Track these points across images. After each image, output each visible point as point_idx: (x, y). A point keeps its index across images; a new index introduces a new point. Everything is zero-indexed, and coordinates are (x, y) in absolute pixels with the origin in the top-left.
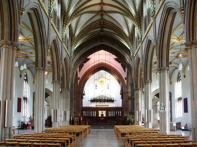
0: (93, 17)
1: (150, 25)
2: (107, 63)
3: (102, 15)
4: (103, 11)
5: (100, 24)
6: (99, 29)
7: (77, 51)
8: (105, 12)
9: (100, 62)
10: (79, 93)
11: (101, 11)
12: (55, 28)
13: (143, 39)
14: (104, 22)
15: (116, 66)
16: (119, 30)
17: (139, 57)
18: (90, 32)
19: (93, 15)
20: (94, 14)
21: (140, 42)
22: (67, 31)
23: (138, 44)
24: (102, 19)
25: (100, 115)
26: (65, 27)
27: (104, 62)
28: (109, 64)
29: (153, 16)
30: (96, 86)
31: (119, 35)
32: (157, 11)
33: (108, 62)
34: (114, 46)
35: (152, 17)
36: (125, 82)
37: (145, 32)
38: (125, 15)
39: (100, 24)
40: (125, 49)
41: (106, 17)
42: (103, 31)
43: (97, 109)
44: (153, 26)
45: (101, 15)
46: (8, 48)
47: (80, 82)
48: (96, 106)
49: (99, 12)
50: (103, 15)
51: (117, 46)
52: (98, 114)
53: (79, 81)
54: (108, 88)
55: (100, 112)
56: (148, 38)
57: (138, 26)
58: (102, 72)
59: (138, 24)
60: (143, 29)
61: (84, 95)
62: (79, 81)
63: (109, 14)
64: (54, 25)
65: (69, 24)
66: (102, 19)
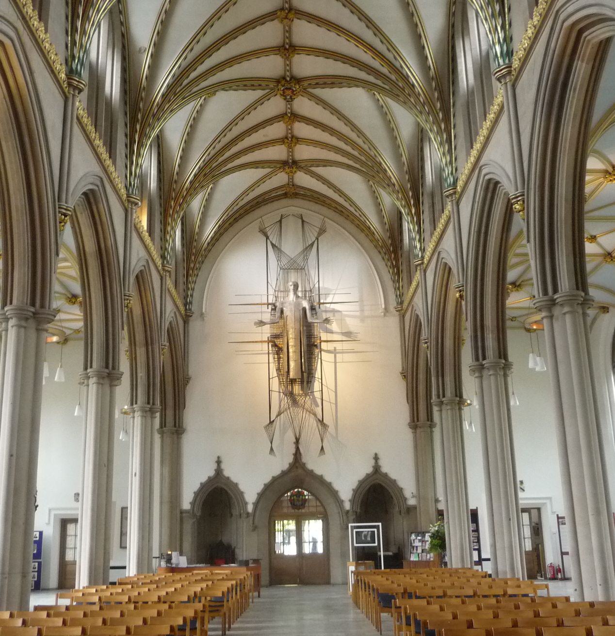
0: (253, 106)
1: (491, 116)
12: (98, 142)
13: (460, 184)
17: (446, 264)
19: (253, 95)
20: (259, 93)
21: (447, 196)
22: (149, 164)
23: (438, 207)
26: (141, 145)
29: (504, 76)
32: (521, 54)
35: (499, 79)
37: (468, 154)
38: (381, 90)
44: (504, 119)
56: (484, 172)
57: (439, 132)
59: (436, 122)
60: (461, 142)
64: (90, 128)
65: (156, 131)
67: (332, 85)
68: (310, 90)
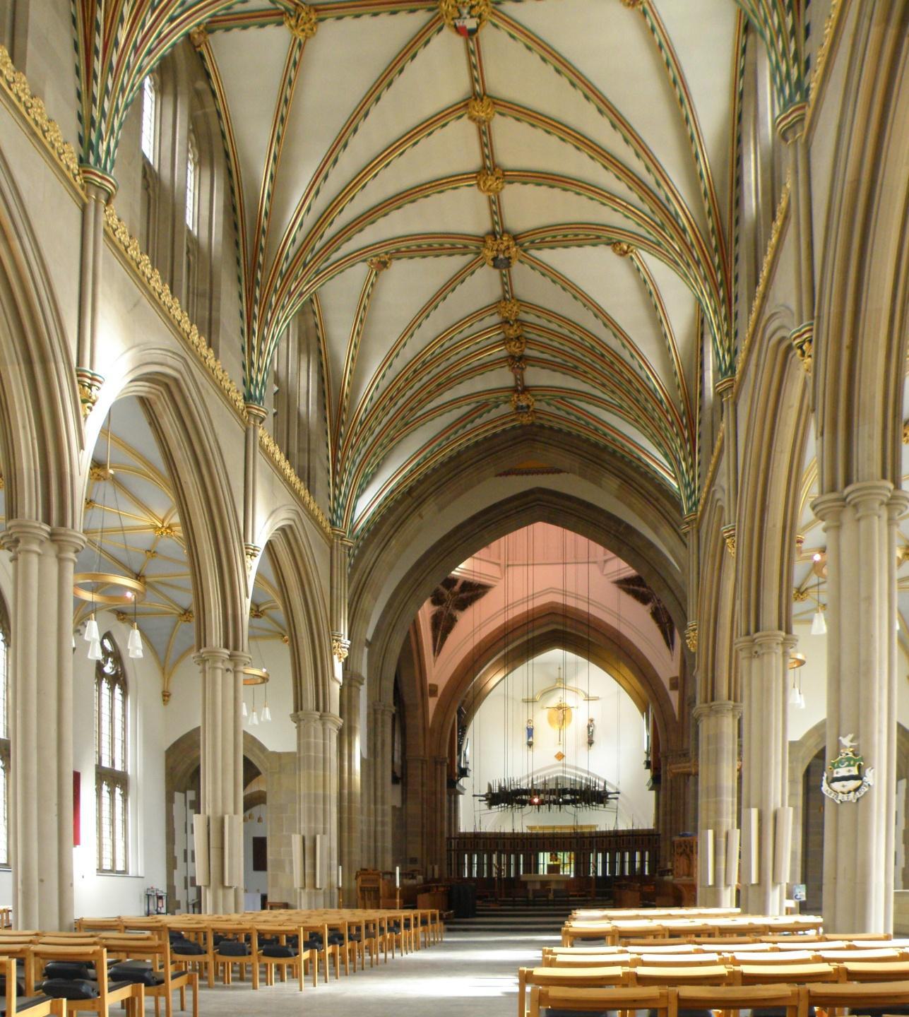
2: (571, 602)
3: (503, 264)
4: (505, 232)
5: (506, 341)
6: (503, 378)
7: (392, 519)
8: (515, 238)
9: (539, 602)
10: (436, 763)
11: (493, 234)
14: (522, 323)
15: (619, 618)
16: (611, 365)
18: (448, 396)
20: (458, 262)
24: (508, 296)
25: (543, 870)
27: (559, 599)
28: (583, 606)
30: (530, 732)
31: (618, 410)
33: (577, 597)
34: (596, 481)
36: (668, 700)
39: (506, 341)
40: (657, 500)
41: (528, 284)
42: (526, 389)
43: (529, 844)
45: (496, 263)
46: (39, 555)
47: (439, 705)
48: (529, 831)
49: (482, 239)
50: (507, 263)
51: (613, 483)
52: (532, 866)
53: (432, 703)
54: (591, 743)
55: (545, 859)
58: (556, 655)
61: (464, 773)
62: (432, 703)
63: (546, 255)
66: (508, 296)
67: (565, 243)
68: (533, 252)
